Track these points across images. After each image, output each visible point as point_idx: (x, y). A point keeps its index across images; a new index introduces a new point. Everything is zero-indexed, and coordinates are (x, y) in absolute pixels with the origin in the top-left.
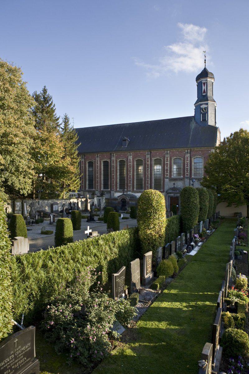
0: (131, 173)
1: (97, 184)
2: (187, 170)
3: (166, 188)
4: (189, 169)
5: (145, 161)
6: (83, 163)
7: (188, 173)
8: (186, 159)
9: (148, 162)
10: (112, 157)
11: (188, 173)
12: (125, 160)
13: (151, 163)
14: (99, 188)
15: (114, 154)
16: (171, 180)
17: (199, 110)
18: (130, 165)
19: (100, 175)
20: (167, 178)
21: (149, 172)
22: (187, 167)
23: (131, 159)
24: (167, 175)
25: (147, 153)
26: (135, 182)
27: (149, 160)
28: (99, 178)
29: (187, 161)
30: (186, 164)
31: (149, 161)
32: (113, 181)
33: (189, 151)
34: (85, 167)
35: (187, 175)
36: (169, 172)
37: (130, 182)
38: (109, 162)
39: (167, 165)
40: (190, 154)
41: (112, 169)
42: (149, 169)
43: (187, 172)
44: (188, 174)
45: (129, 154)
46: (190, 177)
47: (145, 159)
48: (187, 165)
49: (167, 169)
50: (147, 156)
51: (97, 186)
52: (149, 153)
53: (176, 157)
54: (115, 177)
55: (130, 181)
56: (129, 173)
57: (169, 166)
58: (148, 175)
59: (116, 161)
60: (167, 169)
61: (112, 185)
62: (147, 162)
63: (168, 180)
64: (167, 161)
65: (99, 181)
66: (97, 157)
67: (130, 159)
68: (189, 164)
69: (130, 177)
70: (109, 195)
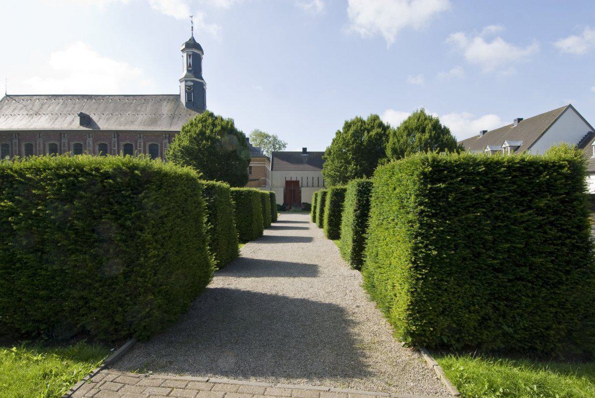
5: (111, 146)
9: (114, 147)
10: (63, 138)
25: (113, 136)
31: (116, 146)
33: (167, 136)
38: (58, 145)
47: (110, 144)
50: (113, 139)
59: (69, 144)
66: (40, 137)
67: (89, 143)
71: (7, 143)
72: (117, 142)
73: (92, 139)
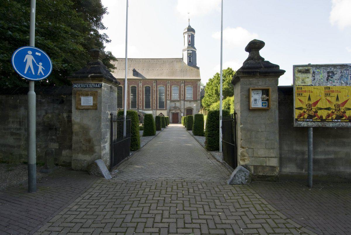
0: (141, 96)
2: (182, 95)
3: (168, 107)
4: (183, 94)
5: (152, 87)
9: (154, 88)
12: (136, 86)
16: (172, 101)
20: (169, 100)
21: (155, 96)
23: (141, 86)
24: (168, 98)
25: (154, 82)
26: (144, 102)
30: (181, 90)
31: (155, 88)
33: (183, 82)
35: (182, 98)
36: (169, 96)
37: (140, 103)
38: (123, 87)
39: (168, 91)
40: (184, 84)
42: (156, 94)
43: (182, 96)
45: (139, 81)
48: (182, 91)
49: (168, 94)
50: (153, 84)
52: (155, 82)
55: (140, 102)
56: (139, 96)
57: (169, 92)
58: (154, 98)
60: (168, 94)
63: (169, 101)
67: (140, 86)
68: (183, 90)
69: (140, 99)
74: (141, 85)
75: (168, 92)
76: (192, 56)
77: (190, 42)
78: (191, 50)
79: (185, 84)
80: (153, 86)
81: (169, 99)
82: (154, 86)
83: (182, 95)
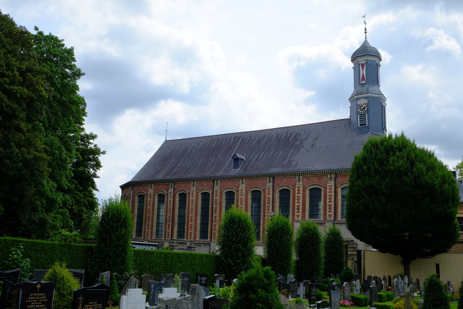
1: (189, 231)
5: (265, 193)
6: (171, 195)
7: (330, 213)
8: (328, 189)
9: (269, 194)
10: (215, 185)
11: (330, 213)
12: (234, 191)
13: (274, 196)
14: (193, 236)
15: (219, 182)
17: (355, 108)
18: (241, 199)
19: (196, 215)
22: (330, 203)
23: (244, 189)
24: (298, 216)
27: (270, 191)
28: (193, 220)
29: (329, 192)
30: (328, 197)
31: (271, 193)
32: (215, 225)
33: (333, 176)
34: (174, 202)
36: (301, 211)
38: (211, 194)
39: (299, 200)
41: (214, 206)
43: (330, 211)
44: (331, 215)
46: (335, 220)
48: (330, 199)
51: (191, 233)
53: (313, 187)
54: (217, 218)
59: (221, 192)
60: (298, 206)
61: (213, 233)
62: (268, 194)
64: (299, 193)
65: (193, 226)
67: (242, 190)
70: (207, 248)
71: (164, 193)
72: (272, 188)
73: (244, 185)
74: (243, 187)
75: (298, 203)
76: (368, 111)
77: (363, 79)
78: (366, 98)
79: (337, 180)
80: (267, 190)
81: (300, 218)
82: (269, 189)
83: (330, 208)
